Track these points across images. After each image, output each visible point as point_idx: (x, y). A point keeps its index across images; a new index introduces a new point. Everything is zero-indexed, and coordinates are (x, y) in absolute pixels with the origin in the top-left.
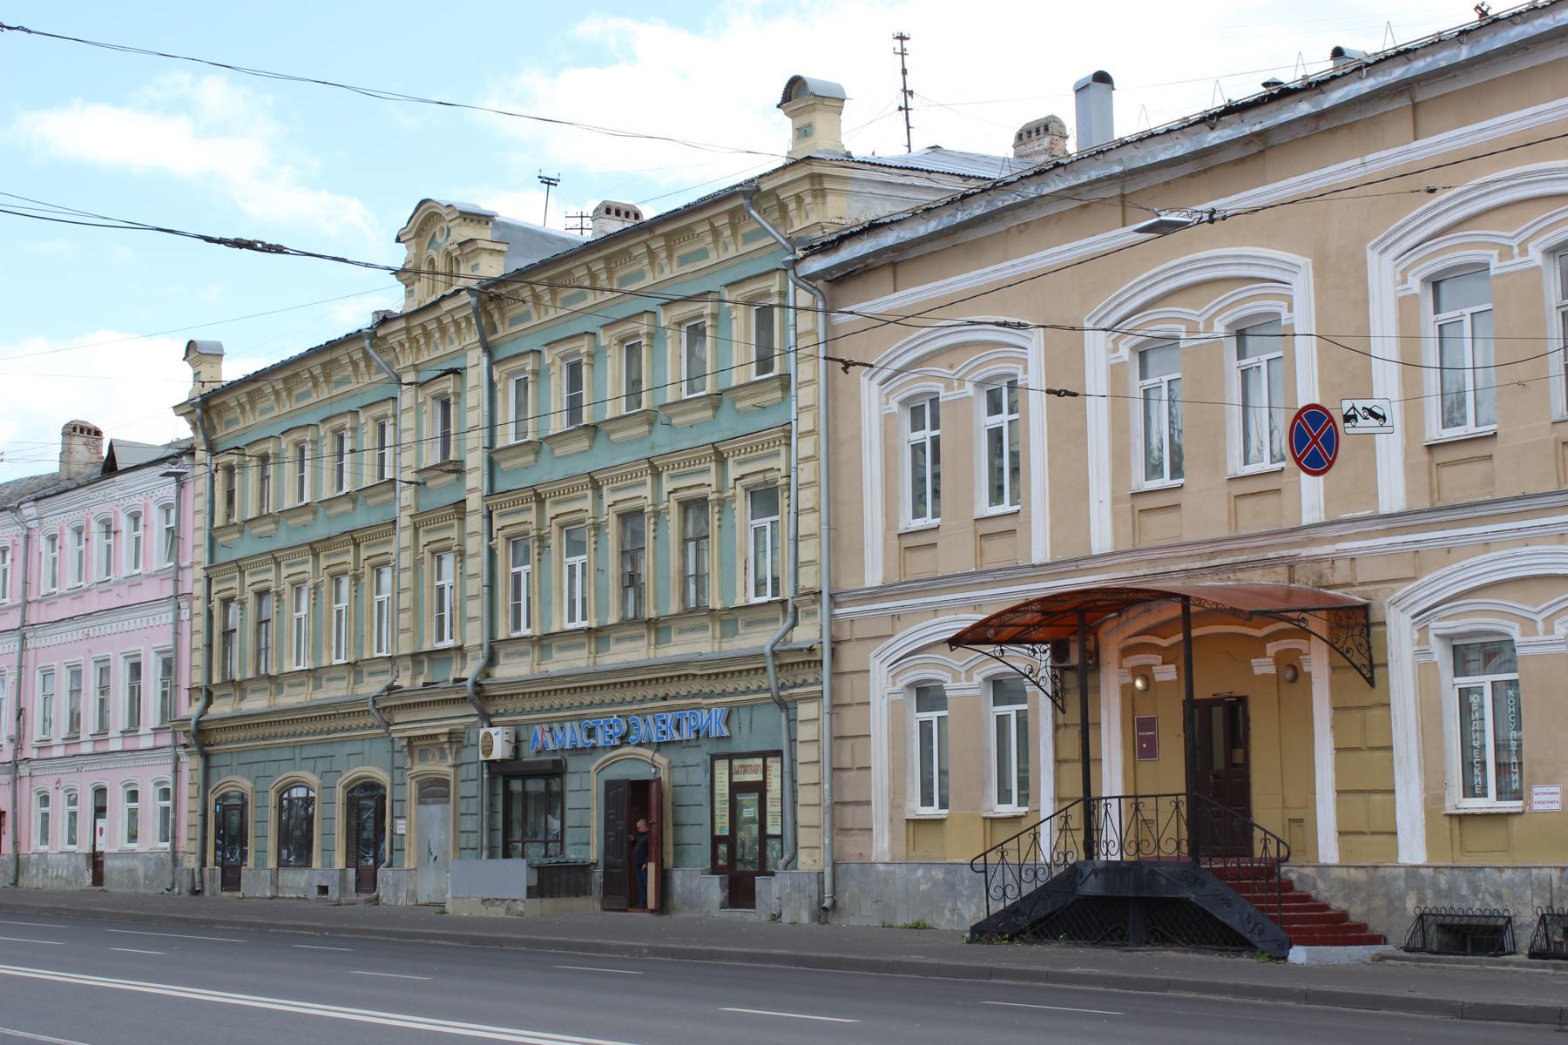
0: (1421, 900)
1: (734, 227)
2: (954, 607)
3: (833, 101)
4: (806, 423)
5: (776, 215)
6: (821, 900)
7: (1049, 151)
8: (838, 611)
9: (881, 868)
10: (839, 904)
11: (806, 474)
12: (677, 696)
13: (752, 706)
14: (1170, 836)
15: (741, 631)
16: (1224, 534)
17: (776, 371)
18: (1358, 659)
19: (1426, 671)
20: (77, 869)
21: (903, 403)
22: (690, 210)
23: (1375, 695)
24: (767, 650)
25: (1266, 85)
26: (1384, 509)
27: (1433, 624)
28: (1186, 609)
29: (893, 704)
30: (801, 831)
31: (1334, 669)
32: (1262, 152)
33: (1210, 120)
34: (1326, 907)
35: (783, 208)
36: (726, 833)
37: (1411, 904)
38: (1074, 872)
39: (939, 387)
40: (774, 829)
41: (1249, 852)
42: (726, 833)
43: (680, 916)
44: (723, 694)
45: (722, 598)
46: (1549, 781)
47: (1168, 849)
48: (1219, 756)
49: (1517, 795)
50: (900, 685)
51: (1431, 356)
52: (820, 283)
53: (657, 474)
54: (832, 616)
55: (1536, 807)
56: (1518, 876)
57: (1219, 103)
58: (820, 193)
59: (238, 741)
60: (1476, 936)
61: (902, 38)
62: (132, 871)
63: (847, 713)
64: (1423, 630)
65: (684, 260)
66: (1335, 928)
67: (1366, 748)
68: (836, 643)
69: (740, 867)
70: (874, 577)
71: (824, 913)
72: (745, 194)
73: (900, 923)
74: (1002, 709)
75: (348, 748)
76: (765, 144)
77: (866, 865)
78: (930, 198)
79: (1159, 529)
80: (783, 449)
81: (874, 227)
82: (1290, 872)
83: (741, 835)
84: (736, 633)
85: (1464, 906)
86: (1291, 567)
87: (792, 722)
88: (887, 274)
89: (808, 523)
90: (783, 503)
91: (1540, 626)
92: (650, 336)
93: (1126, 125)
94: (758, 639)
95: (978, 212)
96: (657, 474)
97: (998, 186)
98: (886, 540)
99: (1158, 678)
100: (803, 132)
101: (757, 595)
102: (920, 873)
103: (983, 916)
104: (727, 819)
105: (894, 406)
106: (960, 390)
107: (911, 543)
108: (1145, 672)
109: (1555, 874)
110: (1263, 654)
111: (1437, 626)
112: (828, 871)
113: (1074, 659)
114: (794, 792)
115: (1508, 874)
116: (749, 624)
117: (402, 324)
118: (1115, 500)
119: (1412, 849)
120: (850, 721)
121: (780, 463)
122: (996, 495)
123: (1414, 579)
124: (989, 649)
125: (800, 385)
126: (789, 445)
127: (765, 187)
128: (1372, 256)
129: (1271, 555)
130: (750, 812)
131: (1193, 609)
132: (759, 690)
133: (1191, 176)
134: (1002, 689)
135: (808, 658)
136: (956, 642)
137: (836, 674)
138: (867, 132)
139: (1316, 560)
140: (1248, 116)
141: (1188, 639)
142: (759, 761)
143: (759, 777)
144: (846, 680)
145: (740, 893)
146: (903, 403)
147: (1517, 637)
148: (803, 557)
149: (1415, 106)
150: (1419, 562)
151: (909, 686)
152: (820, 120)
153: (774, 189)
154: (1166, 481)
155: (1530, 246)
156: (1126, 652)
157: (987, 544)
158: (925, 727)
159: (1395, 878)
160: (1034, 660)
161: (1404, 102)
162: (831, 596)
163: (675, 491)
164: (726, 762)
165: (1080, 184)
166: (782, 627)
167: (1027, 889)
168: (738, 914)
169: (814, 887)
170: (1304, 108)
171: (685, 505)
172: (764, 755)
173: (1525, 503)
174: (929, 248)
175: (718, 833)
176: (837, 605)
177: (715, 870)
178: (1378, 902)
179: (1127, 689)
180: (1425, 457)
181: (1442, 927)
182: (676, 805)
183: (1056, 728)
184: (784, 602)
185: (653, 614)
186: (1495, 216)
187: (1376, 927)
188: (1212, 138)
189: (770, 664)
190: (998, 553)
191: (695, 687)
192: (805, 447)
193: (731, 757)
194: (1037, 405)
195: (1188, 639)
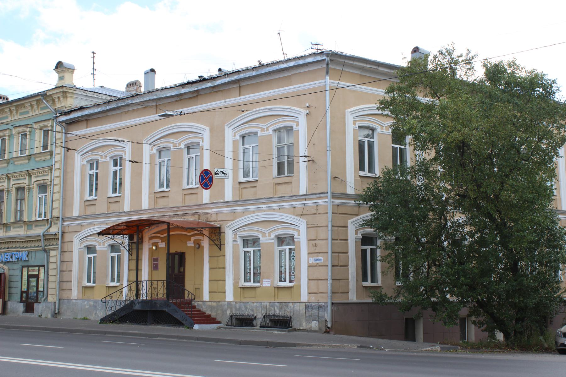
0: (231, 311)
1: (38, 105)
2: (100, 223)
3: (71, 70)
4: (57, 166)
5: (51, 102)
6: (55, 311)
7: (136, 90)
8: (64, 223)
9: (74, 301)
10: (61, 312)
11: (56, 181)
12: (12, 248)
13: (36, 251)
14: (161, 293)
15: (33, 228)
16: (181, 205)
17: (49, 150)
18: (216, 242)
19: (235, 246)
21: (87, 162)
22: (24, 99)
23: (221, 253)
24: (41, 234)
25: (199, 77)
26: (226, 200)
27: (238, 233)
28: (169, 226)
29: (80, 252)
30: (49, 290)
31: (210, 245)
32: (197, 96)
33: (183, 85)
34: (205, 313)
35: (54, 100)
36: (26, 290)
37: (228, 313)
38: (132, 303)
39: (99, 158)
40: (41, 289)
41: (184, 298)
42: (26, 290)
43: (9, 315)
44: (27, 247)
45: (28, 218)
46: (268, 278)
47: (160, 296)
48: (176, 269)
49: (259, 282)
50: (83, 246)
51: (241, 157)
52: (64, 124)
53: (9, 179)
54: (62, 225)
55: (264, 285)
56: (258, 304)
57: (185, 81)
58: (65, 97)
60: (246, 321)
61: (93, 53)
63: (66, 254)
64: (235, 235)
65: (21, 114)
66: (207, 319)
67: (218, 268)
68: (63, 233)
69: (30, 301)
70: (76, 213)
71: (55, 315)
72: (42, 95)
73: (79, 318)
74: (113, 254)
76: (49, 81)
77: (69, 300)
78: (99, 101)
79: (162, 203)
80: (50, 174)
81: (81, 108)
82: (195, 303)
83: (30, 291)
84: (32, 229)
85: (243, 313)
86: (199, 215)
87: (48, 256)
88: (85, 123)
89: (56, 196)
90: (49, 190)
91: (267, 235)
92: (9, 136)
93: (158, 85)
94: (39, 231)
95: (113, 107)
96: (9, 179)
97: (119, 99)
98: (80, 202)
99: (160, 246)
100: (61, 78)
101: (39, 217)
102: (86, 303)
103: (104, 315)
104: (26, 286)
105: (85, 162)
106: (105, 159)
107: (88, 204)
108: (156, 244)
109: (268, 304)
110: (190, 240)
111: (239, 234)
112: (57, 302)
113: (135, 240)
114: (48, 278)
115: (255, 304)
116: (36, 226)
118: (150, 194)
119: (230, 297)
120: (66, 257)
121: (48, 178)
122: (115, 191)
123: (233, 220)
124: (110, 236)
125: (56, 154)
126: (51, 172)
127: (48, 94)
128: (226, 128)
129: (194, 212)
130: (33, 283)
131: (171, 226)
132: (38, 246)
133: (176, 101)
134: (113, 248)
135: (54, 237)
136: (100, 234)
137: (63, 242)
138: (81, 80)
139: (207, 214)
140: (194, 85)
141: (169, 235)
142: (37, 268)
143: (37, 273)
144: (66, 244)
145: (29, 308)
146: (87, 162)
147: (261, 237)
148: (54, 206)
149: (240, 87)
150: (235, 215)
151: (85, 246)
152: (67, 75)
153: (51, 95)
154: (165, 189)
155: (269, 129)
156: (151, 238)
157: (111, 205)
158: (90, 259)
159: (224, 305)
160: (124, 240)
161: (237, 85)
162: (62, 219)
163: (15, 184)
164: (27, 268)
165: (143, 101)
166: (46, 227)
167: (118, 308)
168: (28, 315)
169: (53, 306)
170: (209, 84)
171: (18, 189)
172: (39, 266)
173: (265, 200)
174: (98, 116)
175: (23, 290)
176: (64, 221)
177: (21, 301)
178: (219, 312)
179: (151, 250)
180: (238, 186)
181: (238, 319)
182: (10, 281)
183: (129, 260)
184: (47, 220)
185: (5, 222)
186: (260, 119)
187: (219, 319)
188: (183, 91)
189: (42, 238)
190: (114, 208)
191: (18, 245)
192: (57, 173)
193: (28, 267)
194: (128, 166)
195: (169, 235)
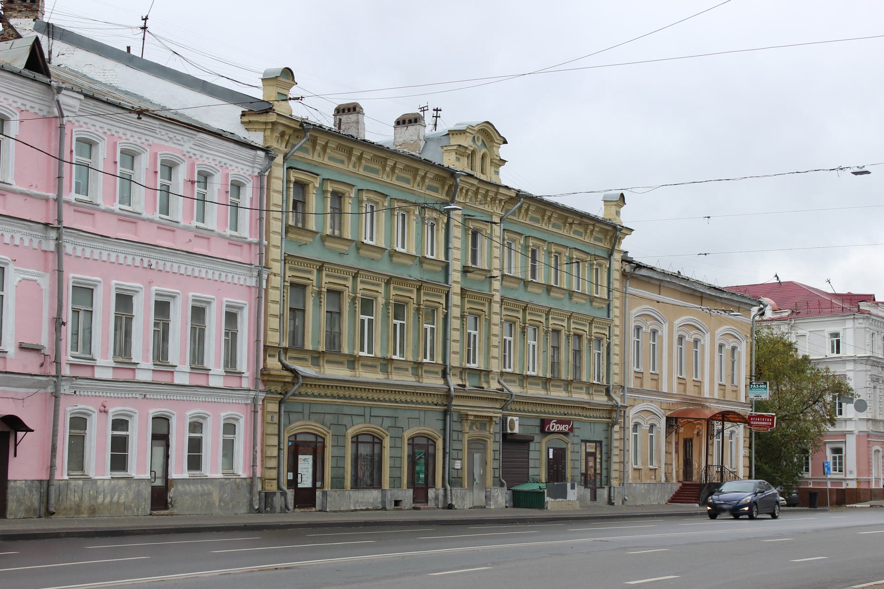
20: (138, 494)
40: (598, 471)
59: (313, 395)
62: (210, 494)
75: (409, 414)
117: (475, 182)
130: (591, 464)
142: (594, 444)
